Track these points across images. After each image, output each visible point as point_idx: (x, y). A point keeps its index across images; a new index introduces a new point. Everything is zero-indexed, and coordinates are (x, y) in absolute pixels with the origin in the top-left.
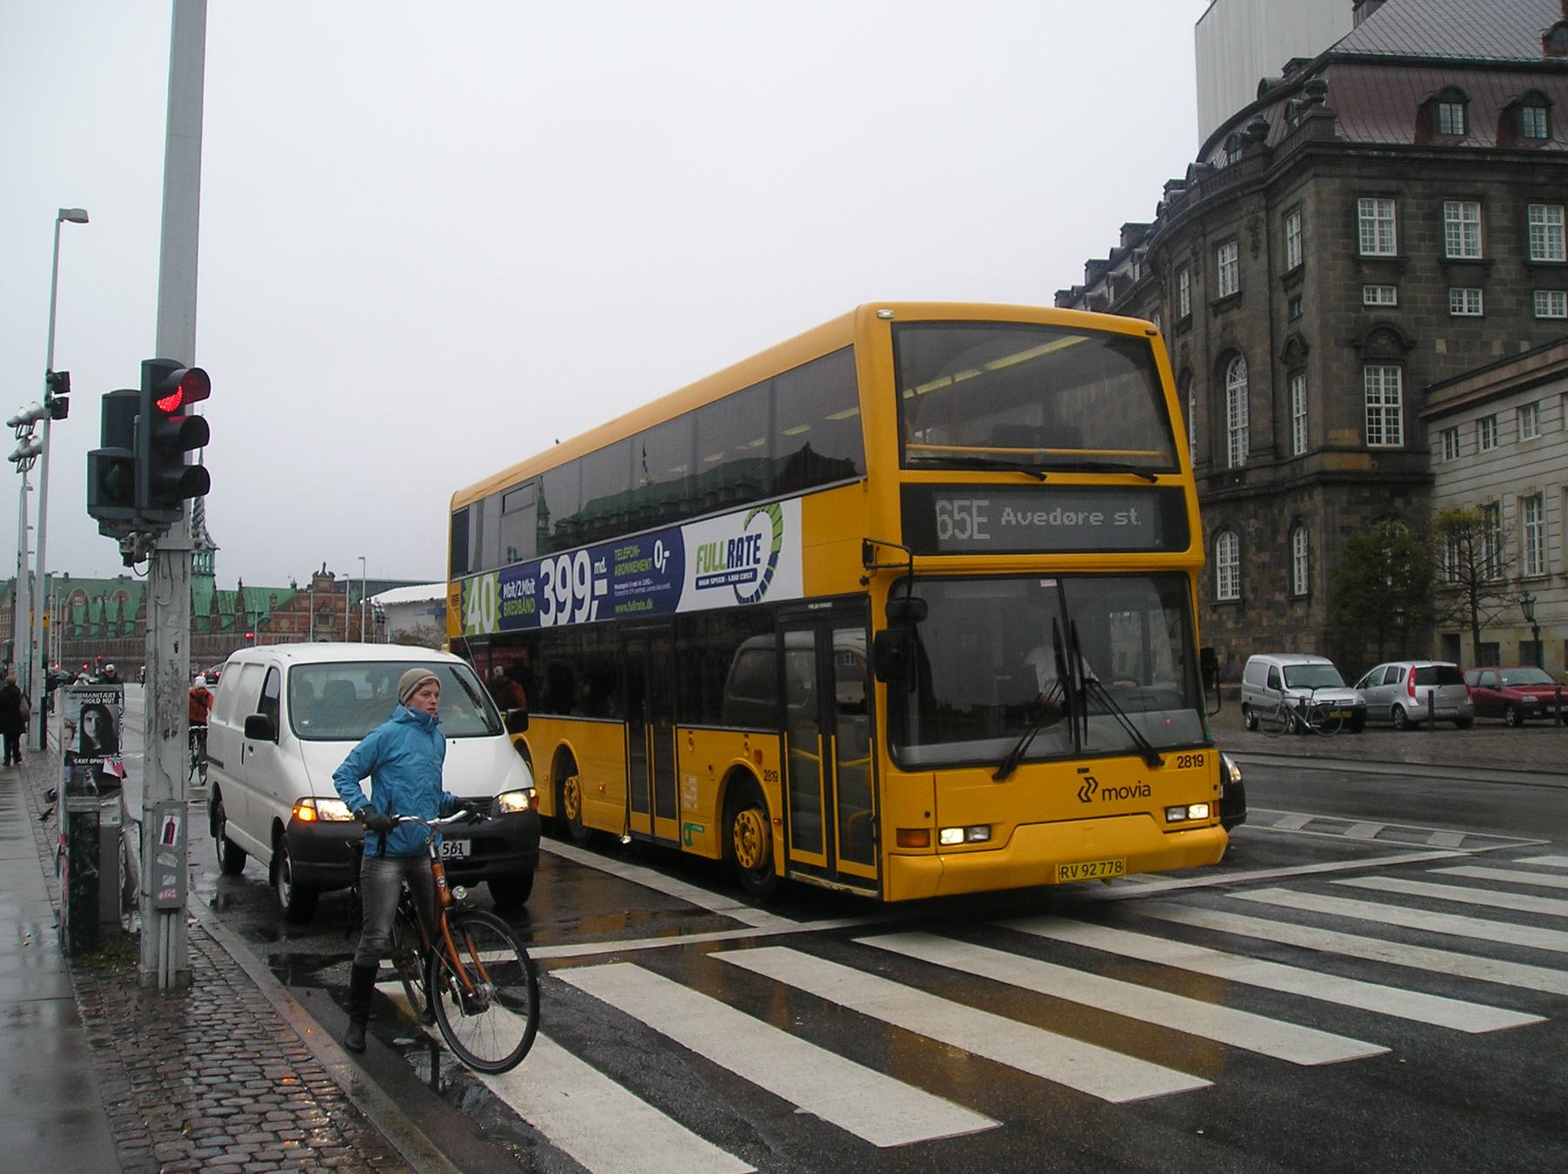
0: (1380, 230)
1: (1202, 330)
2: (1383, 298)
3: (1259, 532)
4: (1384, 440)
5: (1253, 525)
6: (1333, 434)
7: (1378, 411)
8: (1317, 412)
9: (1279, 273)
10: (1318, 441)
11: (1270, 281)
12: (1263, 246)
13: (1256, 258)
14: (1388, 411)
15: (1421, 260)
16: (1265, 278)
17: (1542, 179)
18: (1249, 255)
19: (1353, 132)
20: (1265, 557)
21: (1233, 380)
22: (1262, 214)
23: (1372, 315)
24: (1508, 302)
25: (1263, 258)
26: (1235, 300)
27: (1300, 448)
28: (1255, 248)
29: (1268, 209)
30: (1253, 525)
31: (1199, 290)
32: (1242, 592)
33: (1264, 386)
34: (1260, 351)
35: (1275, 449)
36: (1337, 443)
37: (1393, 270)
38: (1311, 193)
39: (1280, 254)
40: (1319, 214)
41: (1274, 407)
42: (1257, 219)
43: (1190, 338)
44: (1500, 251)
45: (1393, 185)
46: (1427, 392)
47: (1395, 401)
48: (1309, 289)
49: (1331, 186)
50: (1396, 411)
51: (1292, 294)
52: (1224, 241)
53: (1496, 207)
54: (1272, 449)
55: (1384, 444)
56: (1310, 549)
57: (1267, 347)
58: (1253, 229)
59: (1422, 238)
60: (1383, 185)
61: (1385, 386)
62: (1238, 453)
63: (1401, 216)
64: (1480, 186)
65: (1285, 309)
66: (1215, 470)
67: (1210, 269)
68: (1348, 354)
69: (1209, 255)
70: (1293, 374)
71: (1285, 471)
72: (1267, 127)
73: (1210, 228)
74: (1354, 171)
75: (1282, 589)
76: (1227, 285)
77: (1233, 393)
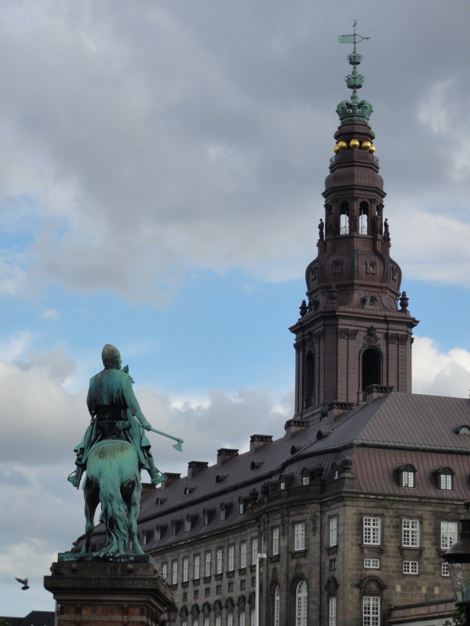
0: (374, 532)
2: (371, 564)
7: (369, 618)
11: (321, 547)
12: (318, 530)
13: (314, 535)
15: (391, 547)
17: (448, 510)
18: (311, 533)
21: (300, 592)
22: (318, 514)
23: (368, 573)
24: (430, 568)
25: (318, 536)
26: (304, 554)
28: (314, 530)
29: (321, 512)
31: (284, 543)
33: (316, 599)
39: (326, 536)
41: (320, 610)
42: (316, 516)
43: (278, 566)
44: (427, 544)
45: (380, 511)
47: (377, 613)
50: (377, 619)
51: (332, 557)
52: (299, 522)
53: (426, 523)
57: (318, 580)
59: (392, 537)
60: (375, 511)
64: (419, 513)
65: (327, 563)
67: (290, 535)
69: (290, 527)
70: (330, 595)
73: (291, 513)
74: (362, 504)
76: (299, 546)
77: (300, 598)
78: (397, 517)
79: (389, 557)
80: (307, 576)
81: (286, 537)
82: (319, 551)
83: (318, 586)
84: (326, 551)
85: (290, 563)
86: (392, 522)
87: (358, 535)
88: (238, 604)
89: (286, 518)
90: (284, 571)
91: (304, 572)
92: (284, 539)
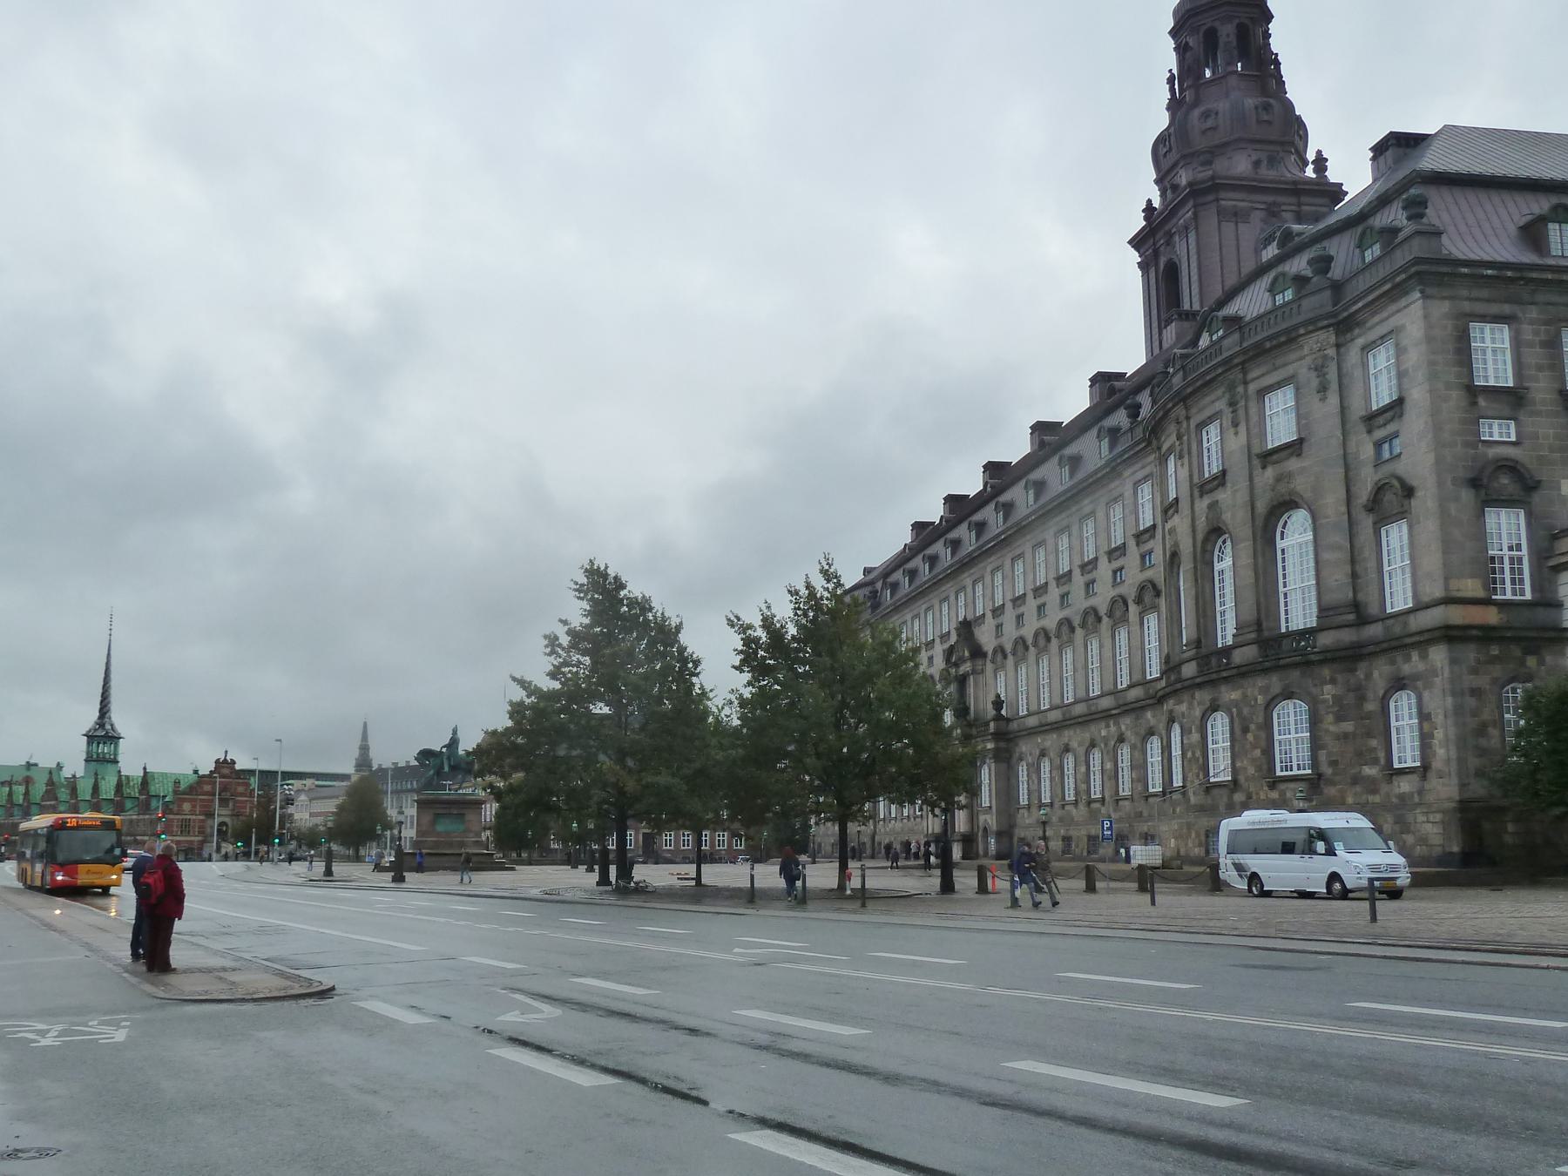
1: (1243, 484)
3: (1337, 699)
4: (1509, 591)
5: (1328, 692)
6: (1454, 584)
8: (1432, 561)
9: (1357, 409)
10: (1435, 590)
12: (1334, 386)
13: (1323, 399)
14: (1512, 559)
15: (1542, 390)
16: (1338, 420)
19: (1457, 246)
20: (1348, 726)
22: (1331, 352)
23: (1492, 452)
25: (1333, 399)
26: (1295, 448)
27: (1399, 598)
28: (1323, 389)
29: (1338, 346)
30: (1328, 692)
31: (1237, 442)
32: (1315, 763)
33: (1340, 538)
34: (1333, 502)
35: (1356, 606)
36: (1460, 594)
37: (1513, 400)
38: (1413, 317)
40: (1429, 339)
41: (1353, 561)
43: (1223, 496)
45: (1507, 309)
46: (1555, 537)
47: (1519, 547)
48: (1415, 425)
49: (1442, 308)
50: (1520, 560)
51: (1379, 434)
54: (1350, 608)
55: (1509, 596)
56: (1424, 716)
57: (1342, 493)
58: (1319, 369)
59: (1540, 368)
60: (1495, 309)
61: (1507, 529)
62: (1298, 612)
63: (1517, 344)
65: (1368, 451)
66: (1266, 634)
67: (1254, 418)
68: (1467, 495)
71: (1374, 631)
72: (1329, 259)
73: (1251, 376)
74: (1465, 293)
75: (1375, 761)
78: (1547, 323)
79: (1539, 414)
80: (1308, 495)
81: (1242, 428)
82: (1339, 433)
83: (1344, 509)
84: (1362, 428)
85: (1257, 480)
86: (1536, 333)
87: (1460, 363)
88: (1110, 614)
89: (1240, 389)
90: (1242, 496)
91: (1298, 488)
92: (1236, 433)
